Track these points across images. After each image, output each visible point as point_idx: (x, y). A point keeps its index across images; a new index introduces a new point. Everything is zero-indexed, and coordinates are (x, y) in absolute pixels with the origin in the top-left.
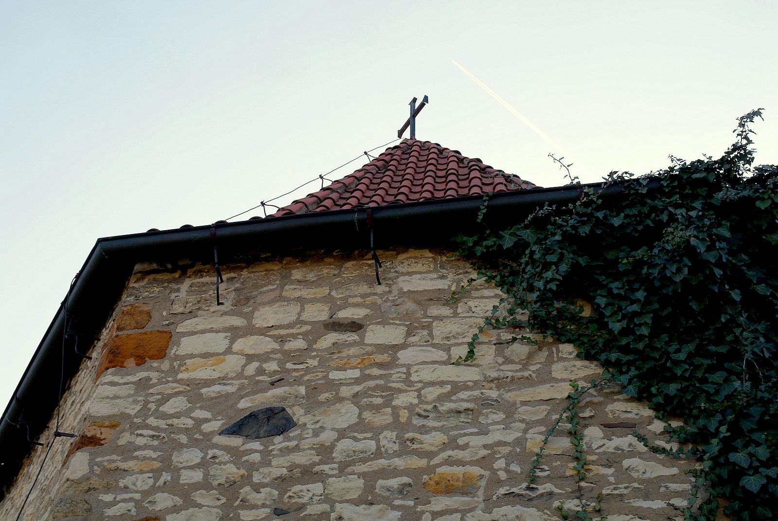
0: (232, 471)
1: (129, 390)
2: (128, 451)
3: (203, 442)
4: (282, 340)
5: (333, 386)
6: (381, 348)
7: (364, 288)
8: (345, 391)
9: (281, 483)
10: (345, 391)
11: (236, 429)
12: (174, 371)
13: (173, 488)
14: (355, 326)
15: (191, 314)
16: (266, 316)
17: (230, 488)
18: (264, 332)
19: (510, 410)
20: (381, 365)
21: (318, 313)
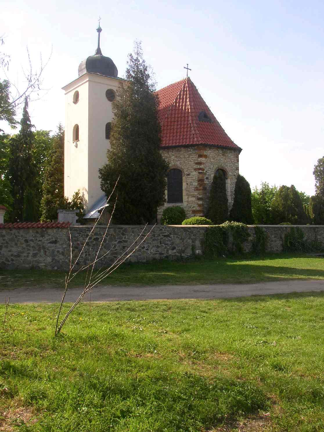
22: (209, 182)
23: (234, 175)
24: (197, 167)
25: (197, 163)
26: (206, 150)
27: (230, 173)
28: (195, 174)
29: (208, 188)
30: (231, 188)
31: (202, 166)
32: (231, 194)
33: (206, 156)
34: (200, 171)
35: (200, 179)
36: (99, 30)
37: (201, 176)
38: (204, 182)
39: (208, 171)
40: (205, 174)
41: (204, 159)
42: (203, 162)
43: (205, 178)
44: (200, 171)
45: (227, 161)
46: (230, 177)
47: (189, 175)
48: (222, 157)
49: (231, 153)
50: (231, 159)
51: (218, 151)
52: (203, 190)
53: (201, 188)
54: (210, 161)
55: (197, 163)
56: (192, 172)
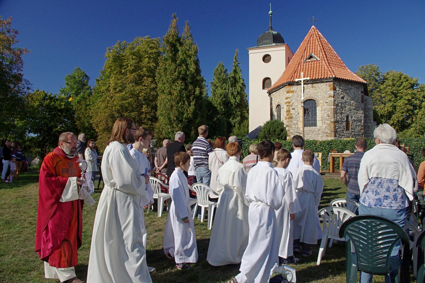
7: (346, 86)
14: (346, 90)
21: (344, 88)
23: (326, 102)
24: (286, 101)
25: (286, 98)
28: (285, 106)
29: (294, 117)
30: (322, 114)
31: (288, 100)
32: (322, 119)
33: (293, 92)
34: (288, 104)
35: (287, 110)
37: (288, 107)
40: (292, 106)
41: (291, 94)
42: (289, 96)
43: (291, 109)
44: (288, 104)
46: (321, 105)
47: (283, 108)
48: (311, 89)
52: (289, 118)
53: (288, 117)
54: (297, 95)
55: (286, 98)
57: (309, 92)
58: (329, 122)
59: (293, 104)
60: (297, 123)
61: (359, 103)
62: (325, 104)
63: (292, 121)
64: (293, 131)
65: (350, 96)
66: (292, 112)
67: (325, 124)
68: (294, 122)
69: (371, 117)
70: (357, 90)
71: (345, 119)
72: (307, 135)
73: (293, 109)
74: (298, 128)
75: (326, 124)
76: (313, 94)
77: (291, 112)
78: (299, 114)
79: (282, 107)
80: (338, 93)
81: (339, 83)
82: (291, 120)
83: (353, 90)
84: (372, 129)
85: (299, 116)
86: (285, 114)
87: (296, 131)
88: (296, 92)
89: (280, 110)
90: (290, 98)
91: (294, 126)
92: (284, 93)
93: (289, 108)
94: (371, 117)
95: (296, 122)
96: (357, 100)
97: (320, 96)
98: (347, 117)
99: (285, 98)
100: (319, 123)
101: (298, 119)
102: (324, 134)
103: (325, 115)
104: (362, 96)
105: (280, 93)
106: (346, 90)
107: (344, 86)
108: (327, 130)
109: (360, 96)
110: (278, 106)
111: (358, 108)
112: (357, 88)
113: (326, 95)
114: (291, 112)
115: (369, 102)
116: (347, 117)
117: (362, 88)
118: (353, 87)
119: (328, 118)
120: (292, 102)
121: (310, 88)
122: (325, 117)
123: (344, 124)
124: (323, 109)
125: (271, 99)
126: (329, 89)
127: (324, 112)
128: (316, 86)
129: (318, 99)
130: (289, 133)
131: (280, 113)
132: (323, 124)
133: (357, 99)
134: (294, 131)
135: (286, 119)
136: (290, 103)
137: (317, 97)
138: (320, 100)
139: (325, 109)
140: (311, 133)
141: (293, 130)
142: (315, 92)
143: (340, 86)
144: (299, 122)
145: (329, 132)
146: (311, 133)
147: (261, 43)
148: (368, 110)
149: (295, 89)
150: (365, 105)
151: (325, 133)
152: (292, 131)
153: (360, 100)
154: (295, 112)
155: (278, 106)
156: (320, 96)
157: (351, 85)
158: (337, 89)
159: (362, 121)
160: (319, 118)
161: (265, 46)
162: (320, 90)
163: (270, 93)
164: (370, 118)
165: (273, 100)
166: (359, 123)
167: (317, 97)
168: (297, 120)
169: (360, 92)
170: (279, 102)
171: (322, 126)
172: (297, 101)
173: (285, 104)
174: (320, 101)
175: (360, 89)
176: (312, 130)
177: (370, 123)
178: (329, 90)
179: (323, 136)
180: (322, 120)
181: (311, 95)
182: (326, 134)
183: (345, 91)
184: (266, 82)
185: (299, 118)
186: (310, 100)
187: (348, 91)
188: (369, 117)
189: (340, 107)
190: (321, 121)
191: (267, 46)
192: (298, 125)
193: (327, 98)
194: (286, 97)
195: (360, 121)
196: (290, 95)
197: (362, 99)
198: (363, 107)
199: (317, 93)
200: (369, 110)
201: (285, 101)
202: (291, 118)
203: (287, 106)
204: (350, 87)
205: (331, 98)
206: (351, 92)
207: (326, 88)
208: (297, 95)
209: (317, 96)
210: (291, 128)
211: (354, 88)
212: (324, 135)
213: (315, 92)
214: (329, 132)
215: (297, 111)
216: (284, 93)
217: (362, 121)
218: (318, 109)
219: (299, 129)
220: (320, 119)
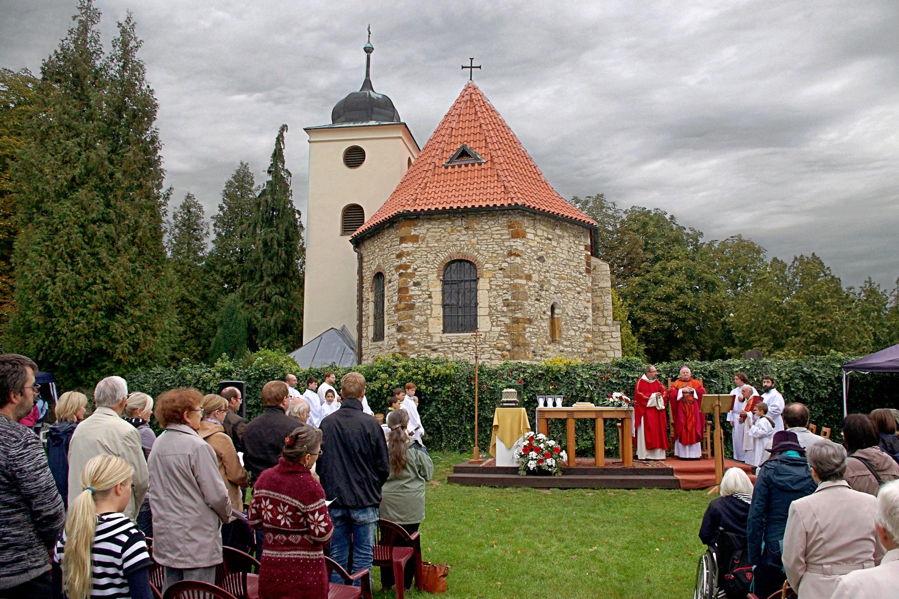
0: (538, 268)
1: (521, 244)
2: (525, 259)
3: (534, 260)
4: (541, 239)
5: (549, 253)
6: (554, 247)
7: (551, 230)
8: (551, 255)
9: (545, 272)
10: (551, 255)
11: (538, 259)
12: (527, 242)
13: (532, 269)
14: (550, 240)
15: (528, 227)
16: (540, 233)
17: (539, 271)
18: (538, 236)
19: (570, 266)
20: (555, 251)
22: (424, 291)
23: (501, 269)
26: (415, 225)
27: (487, 266)
29: (417, 304)
30: (492, 299)
32: (490, 312)
33: (415, 239)
34: (401, 271)
36: (368, 50)
38: (408, 292)
39: (420, 269)
40: (412, 275)
41: (410, 244)
42: (405, 250)
43: (411, 283)
44: (401, 271)
45: (478, 240)
47: (390, 282)
48: (464, 232)
49: (493, 220)
50: (492, 234)
51: (453, 222)
54: (427, 247)
56: (393, 275)
57: (457, 240)
58: (507, 321)
59: (415, 270)
60: (426, 321)
61: (580, 273)
62: (500, 274)
63: (412, 317)
64: (415, 342)
65: (560, 255)
66: (414, 291)
67: (497, 326)
68: (417, 318)
69: (606, 310)
70: (577, 242)
71: (549, 313)
72: (453, 352)
73: (416, 284)
74: (428, 334)
75: (500, 326)
76: (467, 246)
77: (411, 293)
78: (430, 297)
79: (387, 278)
80: (531, 247)
81: (532, 222)
82: (410, 312)
83: (567, 242)
84: (611, 340)
85: (431, 303)
86: (396, 298)
87: (422, 342)
88: (423, 240)
89: (383, 287)
90: (408, 254)
91: (418, 331)
92: (392, 240)
93: (406, 282)
94: (606, 310)
95: (424, 318)
96: (575, 267)
97: (485, 253)
98: (553, 308)
99: (394, 256)
100: (484, 323)
101: (428, 312)
102: (495, 351)
103: (500, 301)
104: (587, 257)
105: (383, 242)
106: (550, 240)
107: (545, 228)
108: (504, 342)
109: (583, 258)
110: (379, 276)
111: (578, 286)
112: (575, 236)
113: (502, 249)
114: (411, 293)
115: (603, 273)
116: (553, 308)
117: (586, 237)
118: (566, 234)
119: (505, 309)
120: (414, 266)
121: (460, 231)
122: (499, 308)
123: (546, 325)
124: (494, 287)
125: (361, 259)
126: (508, 234)
127: (495, 293)
128: (476, 226)
129: (480, 259)
130: (405, 348)
131: (383, 295)
132: (493, 325)
133: (575, 264)
134: (418, 343)
135: (397, 310)
136: (406, 267)
137: (479, 253)
138: (487, 263)
139: (497, 286)
140: (463, 349)
141: (415, 339)
142: (474, 241)
143: (535, 228)
144: (430, 320)
145: (509, 347)
146: (463, 349)
147: (343, 118)
148: (599, 293)
149: (420, 231)
150: (594, 280)
151: (499, 350)
152: (410, 343)
153: (583, 268)
154: (420, 293)
155: (379, 276)
156: (485, 253)
157: (561, 229)
158: (529, 236)
159: (590, 320)
160: (482, 311)
161: (351, 125)
162: (486, 237)
163: (358, 242)
164: (606, 313)
165: (366, 259)
166: (582, 326)
167: (479, 253)
168: (426, 314)
169: (582, 248)
170: (379, 266)
171: (491, 331)
172: (427, 262)
173: (394, 272)
174: (487, 266)
175: (583, 240)
176: (465, 341)
177: (606, 325)
178: (508, 237)
179: (493, 357)
180: (490, 315)
181: (462, 249)
182: (500, 353)
183: (548, 241)
184: (353, 214)
185: (432, 310)
186: (460, 261)
187: (554, 243)
188: (602, 312)
189: (536, 282)
190: (488, 318)
191: (356, 125)
192: (427, 326)
193: (504, 256)
194: (398, 253)
195: (584, 318)
196: (408, 246)
197: (588, 264)
198: (590, 285)
199: (478, 244)
200: (602, 291)
201: (396, 264)
202: (412, 307)
203: (401, 275)
204: (560, 233)
205: (512, 258)
206: (562, 245)
207: (502, 232)
208: (427, 247)
209: (477, 251)
210: (409, 334)
211: (569, 236)
212: (495, 354)
213: (474, 241)
214: (509, 347)
215: (427, 290)
216: (392, 240)
217: (590, 320)
218: (483, 284)
219: (432, 339)
220: (487, 311)
